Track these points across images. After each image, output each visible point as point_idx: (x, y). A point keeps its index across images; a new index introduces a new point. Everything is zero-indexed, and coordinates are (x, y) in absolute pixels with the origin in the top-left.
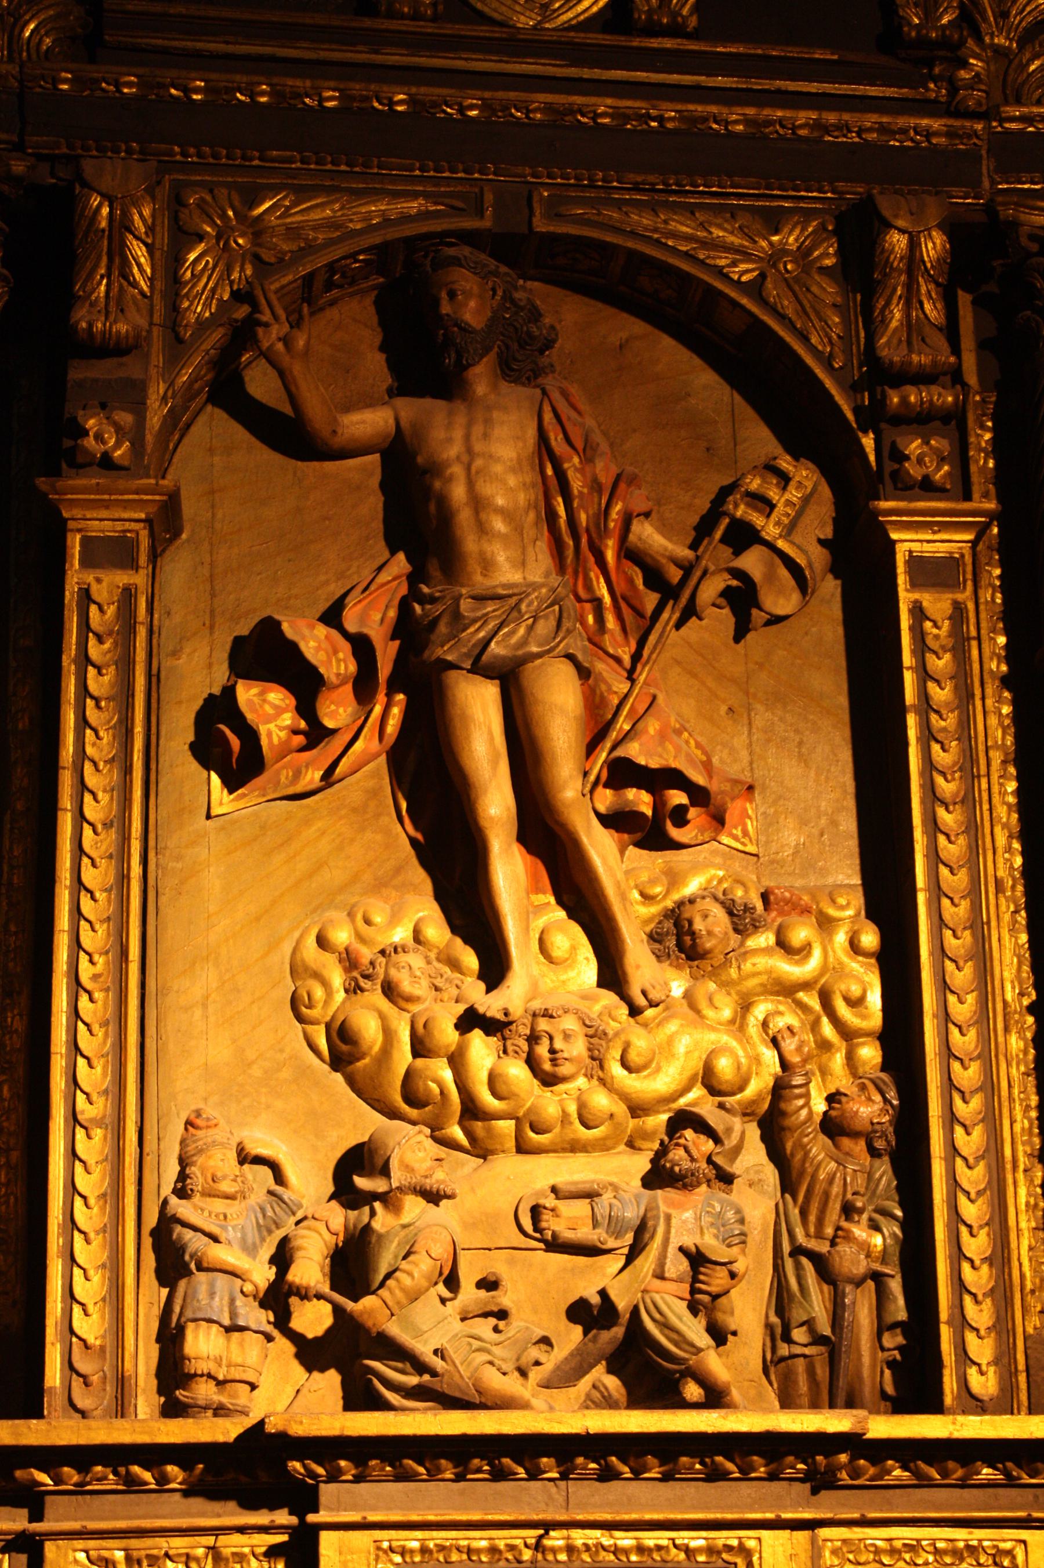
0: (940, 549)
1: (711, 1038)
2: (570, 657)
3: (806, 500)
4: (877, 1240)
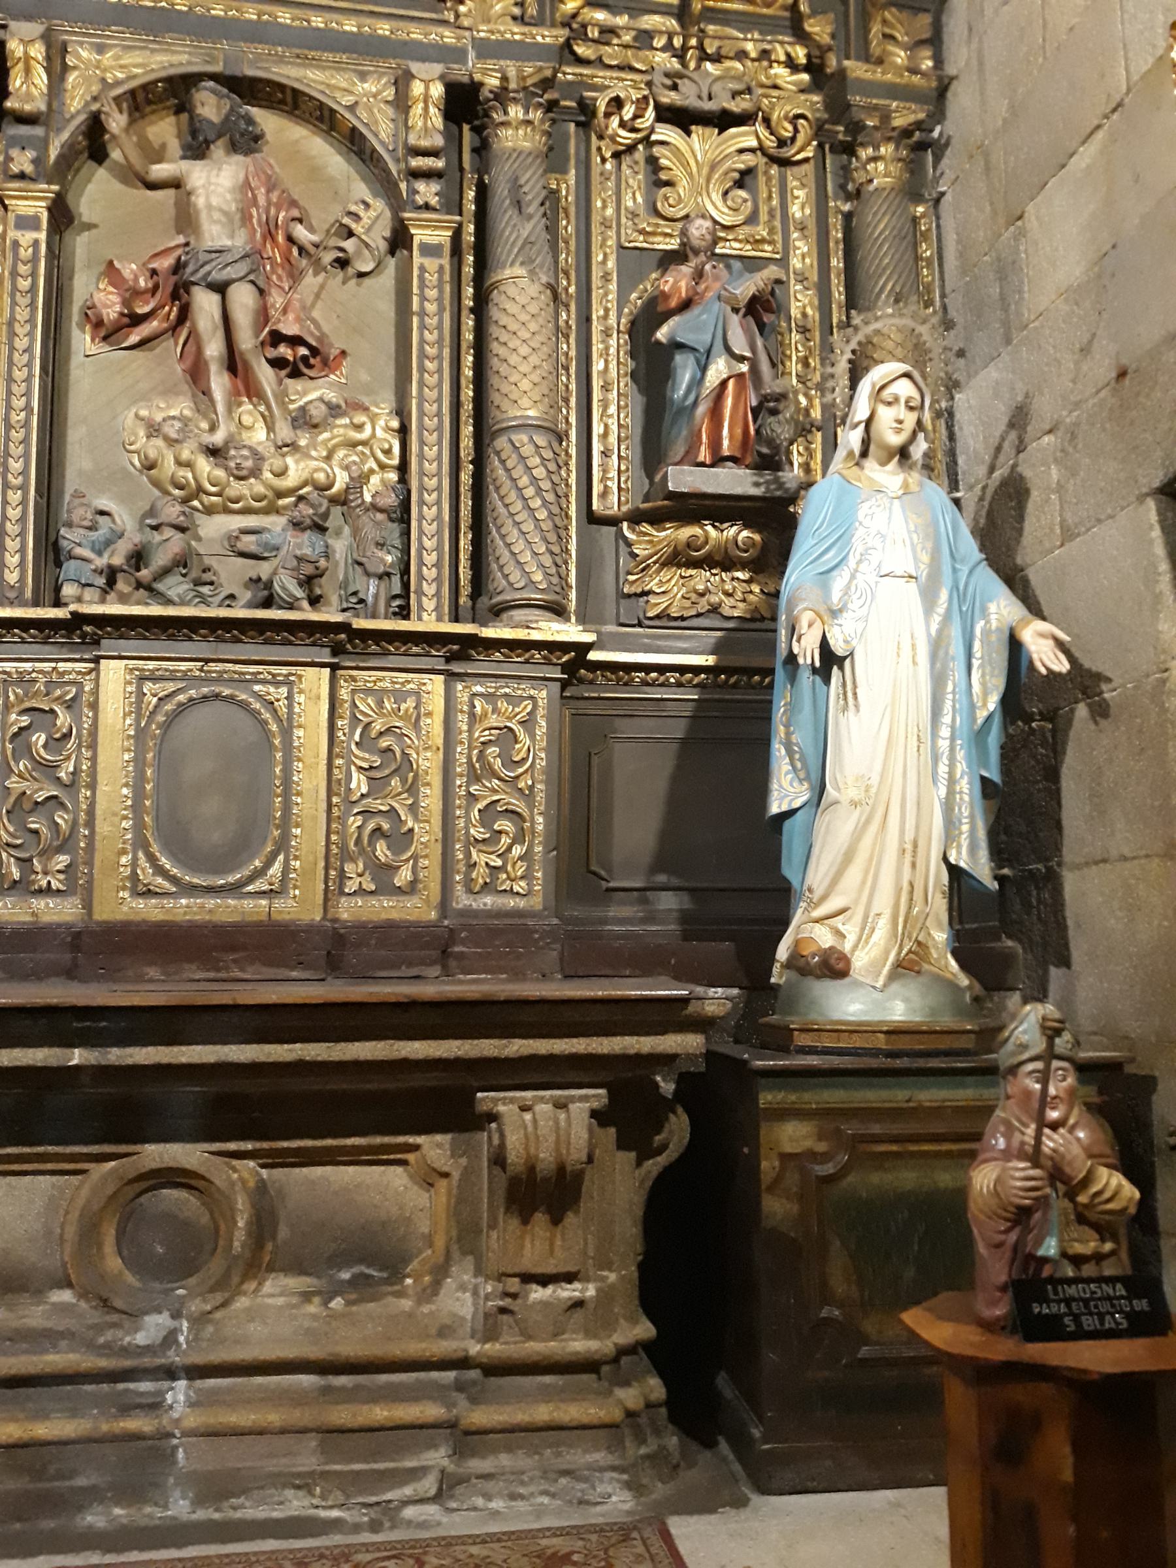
0: (435, 240)
1: (314, 464)
2: (252, 282)
3: (377, 217)
4: (389, 559)
